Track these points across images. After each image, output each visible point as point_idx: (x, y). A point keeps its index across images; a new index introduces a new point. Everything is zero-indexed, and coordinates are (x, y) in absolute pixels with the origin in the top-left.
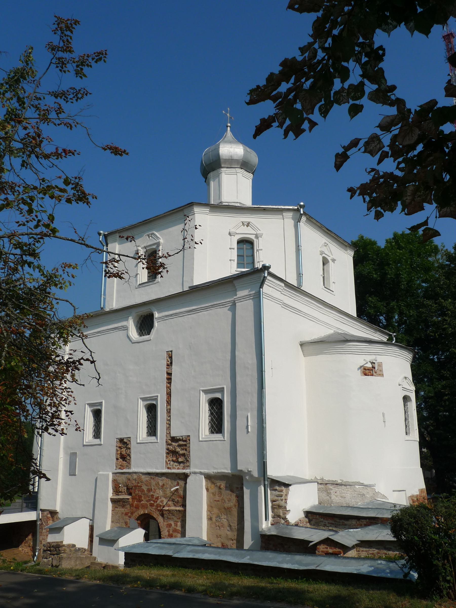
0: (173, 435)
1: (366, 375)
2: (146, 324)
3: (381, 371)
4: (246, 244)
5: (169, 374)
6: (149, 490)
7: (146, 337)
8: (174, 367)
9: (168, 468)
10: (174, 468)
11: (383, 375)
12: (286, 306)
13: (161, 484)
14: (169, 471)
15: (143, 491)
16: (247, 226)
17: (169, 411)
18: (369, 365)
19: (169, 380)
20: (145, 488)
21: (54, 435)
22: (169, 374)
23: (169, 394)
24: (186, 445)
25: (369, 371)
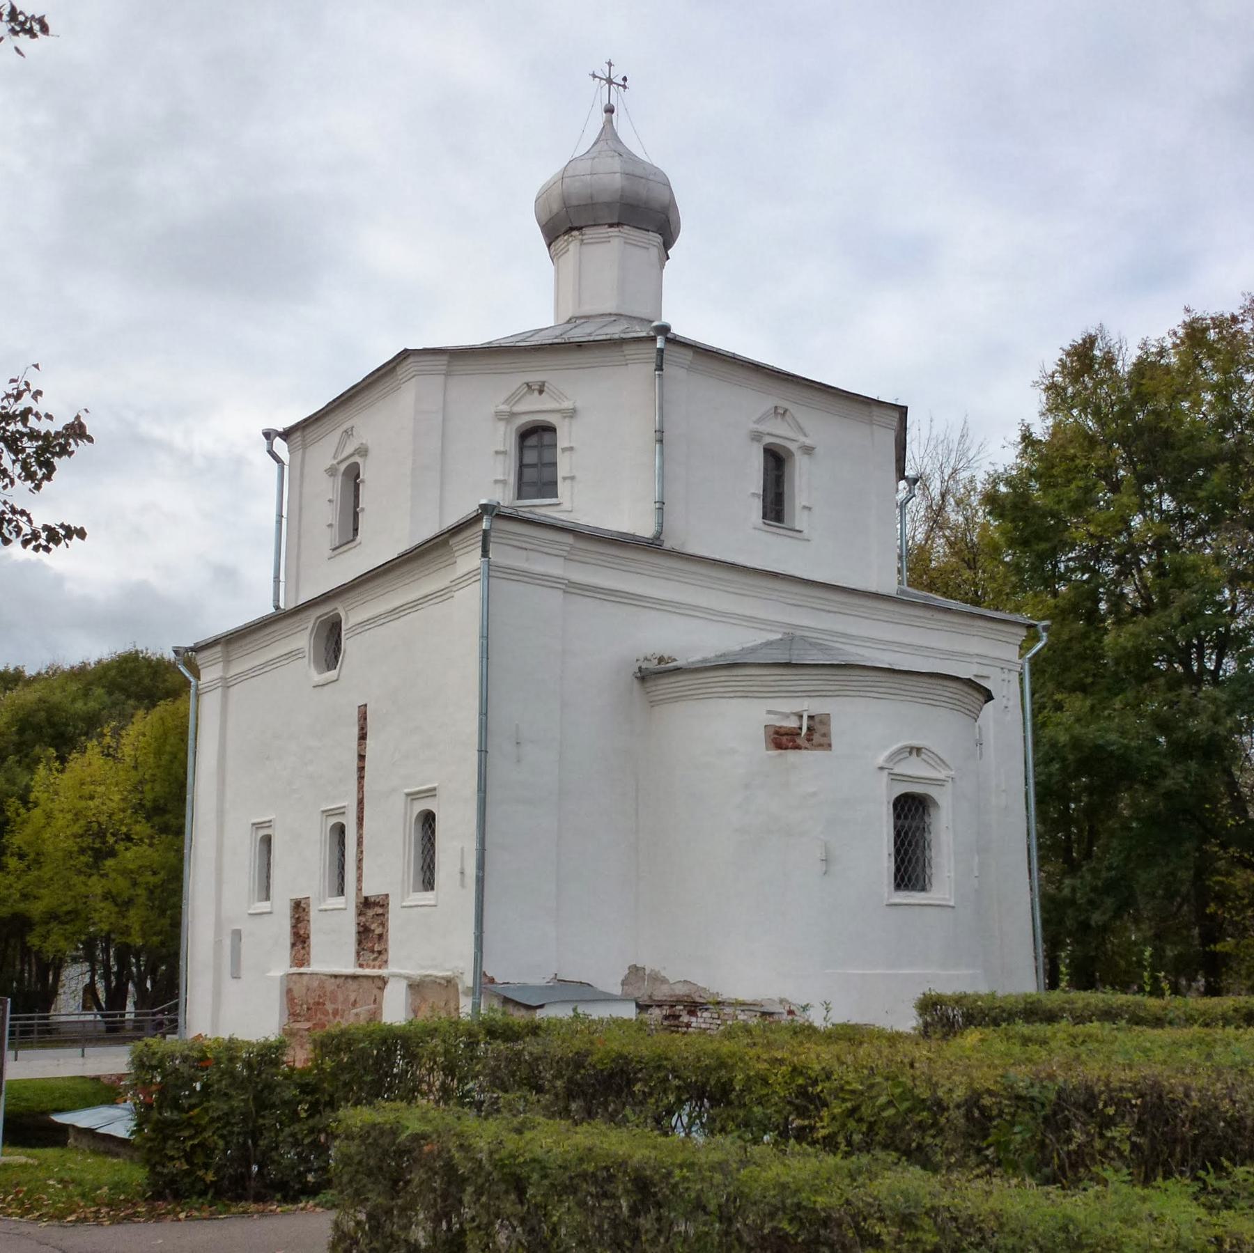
0: (365, 893)
1: (779, 746)
2: (331, 643)
3: (824, 735)
4: (535, 438)
5: (362, 757)
6: (336, 1013)
7: (332, 674)
8: (369, 741)
9: (361, 966)
10: (368, 966)
11: (830, 745)
12: (572, 588)
13: (352, 998)
14: (360, 971)
15: (326, 1013)
16: (541, 392)
17: (360, 843)
18: (792, 723)
19: (361, 769)
20: (329, 1007)
21: (463, 885)
22: (362, 757)
23: (361, 802)
24: (383, 915)
25: (783, 739)
